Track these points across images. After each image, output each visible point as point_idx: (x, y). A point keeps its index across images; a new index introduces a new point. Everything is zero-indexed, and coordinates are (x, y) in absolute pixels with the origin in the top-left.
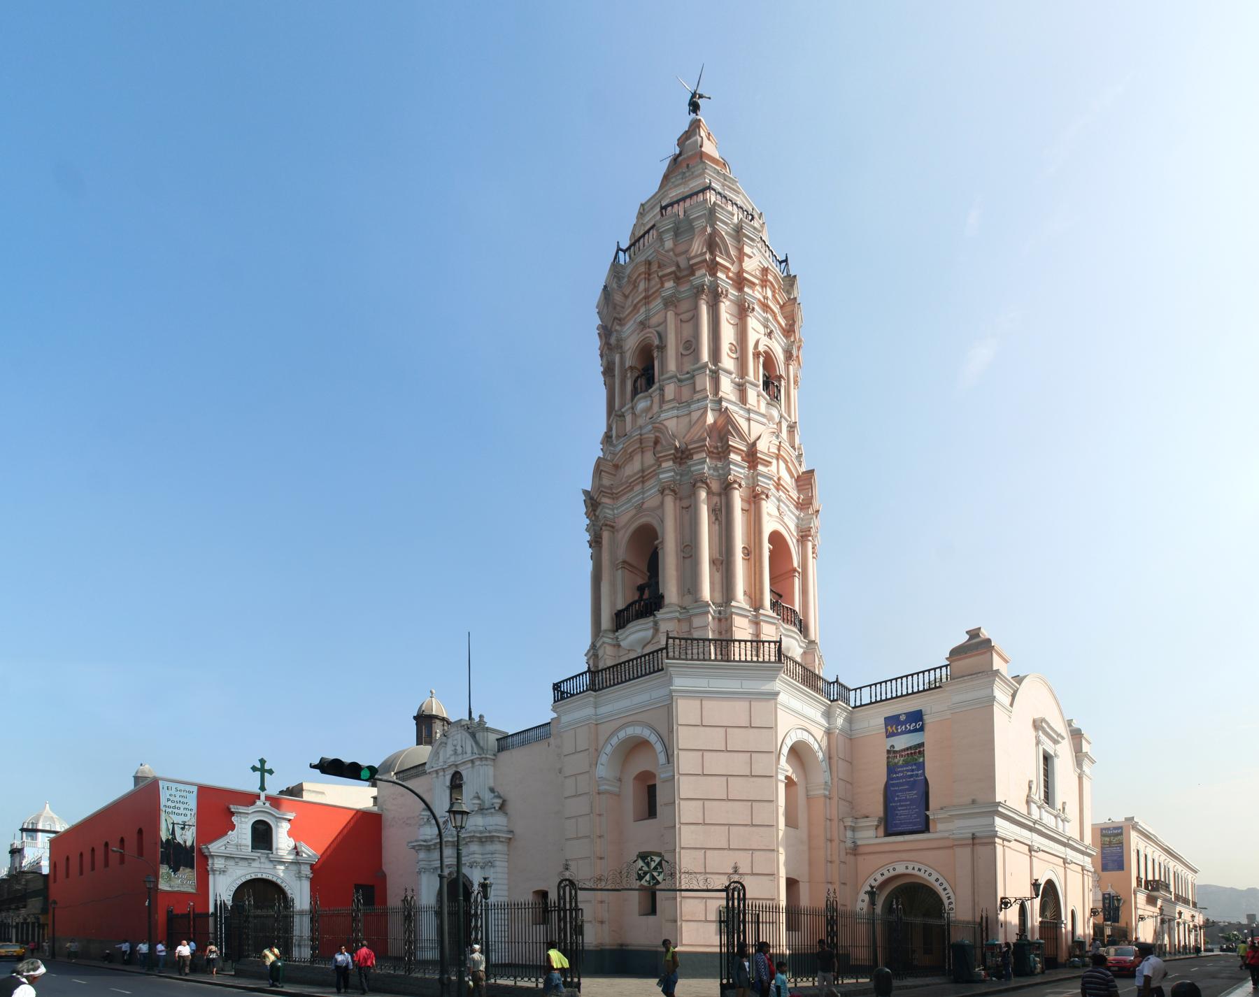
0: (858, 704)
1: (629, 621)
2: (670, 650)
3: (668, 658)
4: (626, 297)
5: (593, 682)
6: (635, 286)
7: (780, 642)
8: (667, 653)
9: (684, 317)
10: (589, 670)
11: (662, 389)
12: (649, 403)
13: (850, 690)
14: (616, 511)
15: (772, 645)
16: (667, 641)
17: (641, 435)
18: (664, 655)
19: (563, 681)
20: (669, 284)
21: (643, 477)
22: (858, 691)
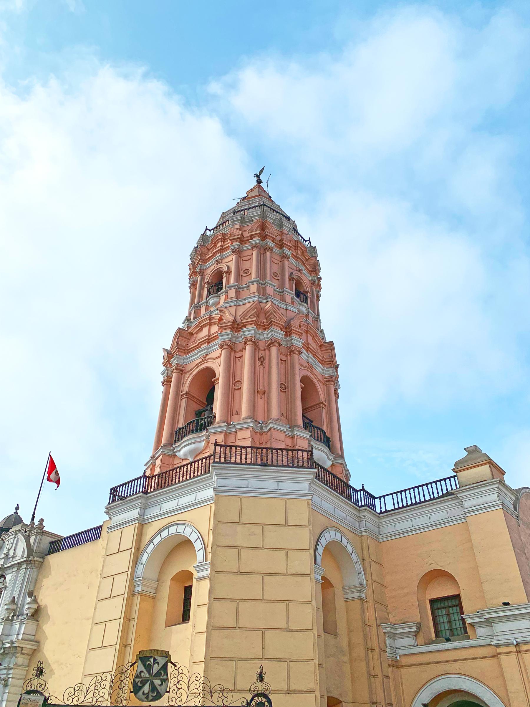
0: (383, 510)
1: (186, 435)
2: (217, 456)
3: (214, 462)
4: (209, 250)
5: (147, 487)
6: (215, 245)
7: (312, 451)
8: (215, 457)
9: (244, 259)
10: (144, 476)
11: (227, 292)
12: (218, 299)
13: (375, 498)
14: (185, 360)
15: (305, 453)
16: (215, 448)
18: (212, 461)
20: (236, 244)
21: (209, 339)
22: (382, 499)
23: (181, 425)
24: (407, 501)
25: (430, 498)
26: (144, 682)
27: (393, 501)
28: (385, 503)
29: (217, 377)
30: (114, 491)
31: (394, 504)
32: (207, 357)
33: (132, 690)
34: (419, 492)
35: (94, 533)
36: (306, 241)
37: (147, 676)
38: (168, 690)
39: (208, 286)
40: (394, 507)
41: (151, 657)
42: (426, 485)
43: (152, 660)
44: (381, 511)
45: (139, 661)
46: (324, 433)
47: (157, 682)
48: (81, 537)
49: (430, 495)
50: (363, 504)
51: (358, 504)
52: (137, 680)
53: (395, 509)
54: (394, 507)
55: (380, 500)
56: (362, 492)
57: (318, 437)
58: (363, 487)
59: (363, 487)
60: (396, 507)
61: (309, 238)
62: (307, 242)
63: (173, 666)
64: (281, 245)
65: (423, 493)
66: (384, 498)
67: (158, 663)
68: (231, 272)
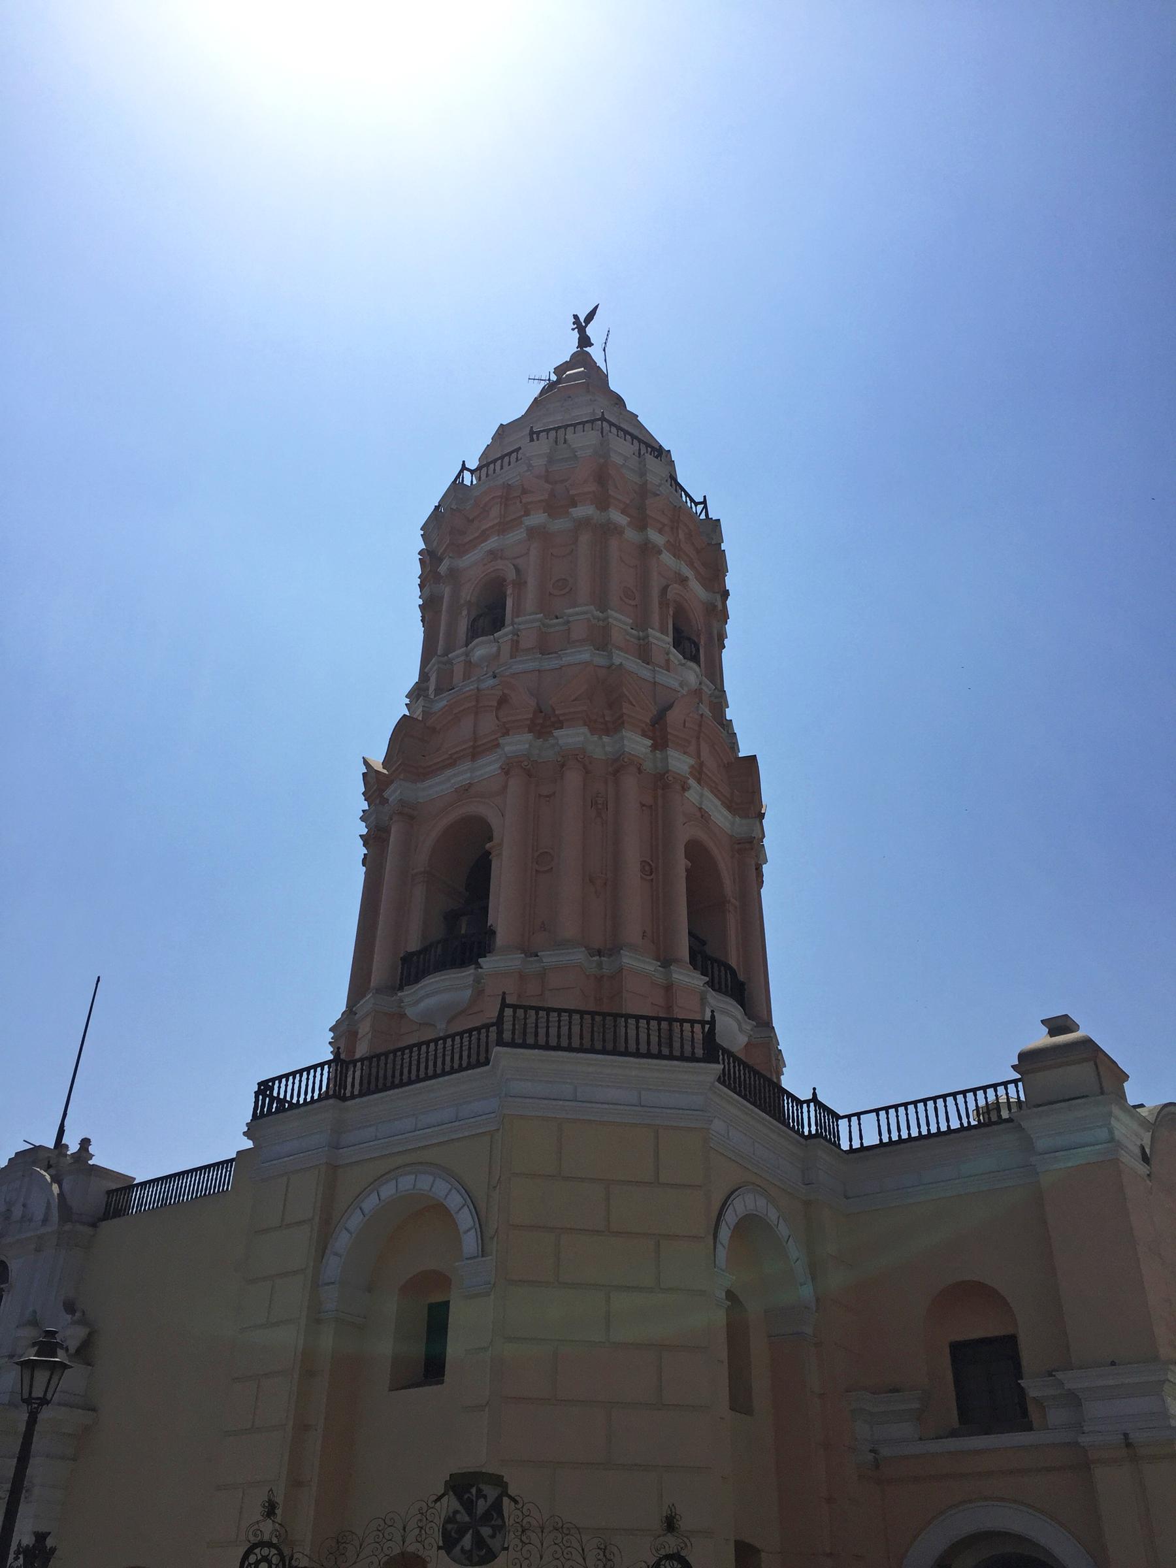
12: (495, 649)
13: (838, 1117)
17: (478, 689)
19: (280, 1078)
23: (414, 945)
24: (909, 1128)
25: (962, 1124)
26: (462, 1532)
27: (879, 1126)
28: (860, 1130)
29: (496, 841)
30: (264, 1088)
31: (880, 1134)
33: (441, 1544)
34: (936, 1109)
35: (213, 1175)
36: (697, 504)
37: (467, 1519)
38: (506, 1545)
39: (469, 614)
40: (881, 1140)
41: (472, 1486)
42: (954, 1095)
43: (474, 1490)
44: (851, 1146)
45: (451, 1493)
46: (733, 973)
47: (486, 1531)
48: (182, 1183)
49: (960, 1118)
50: (814, 1132)
51: (803, 1132)
52: (449, 1526)
53: (882, 1144)
54: (881, 1140)
55: (850, 1121)
56: (812, 1105)
57: (720, 983)
58: (814, 1094)
59: (814, 1094)
60: (885, 1139)
61: (705, 497)
62: (700, 507)
63: (513, 1503)
64: (641, 524)
65: (947, 1113)
66: (859, 1119)
67: (485, 1497)
68: (526, 582)
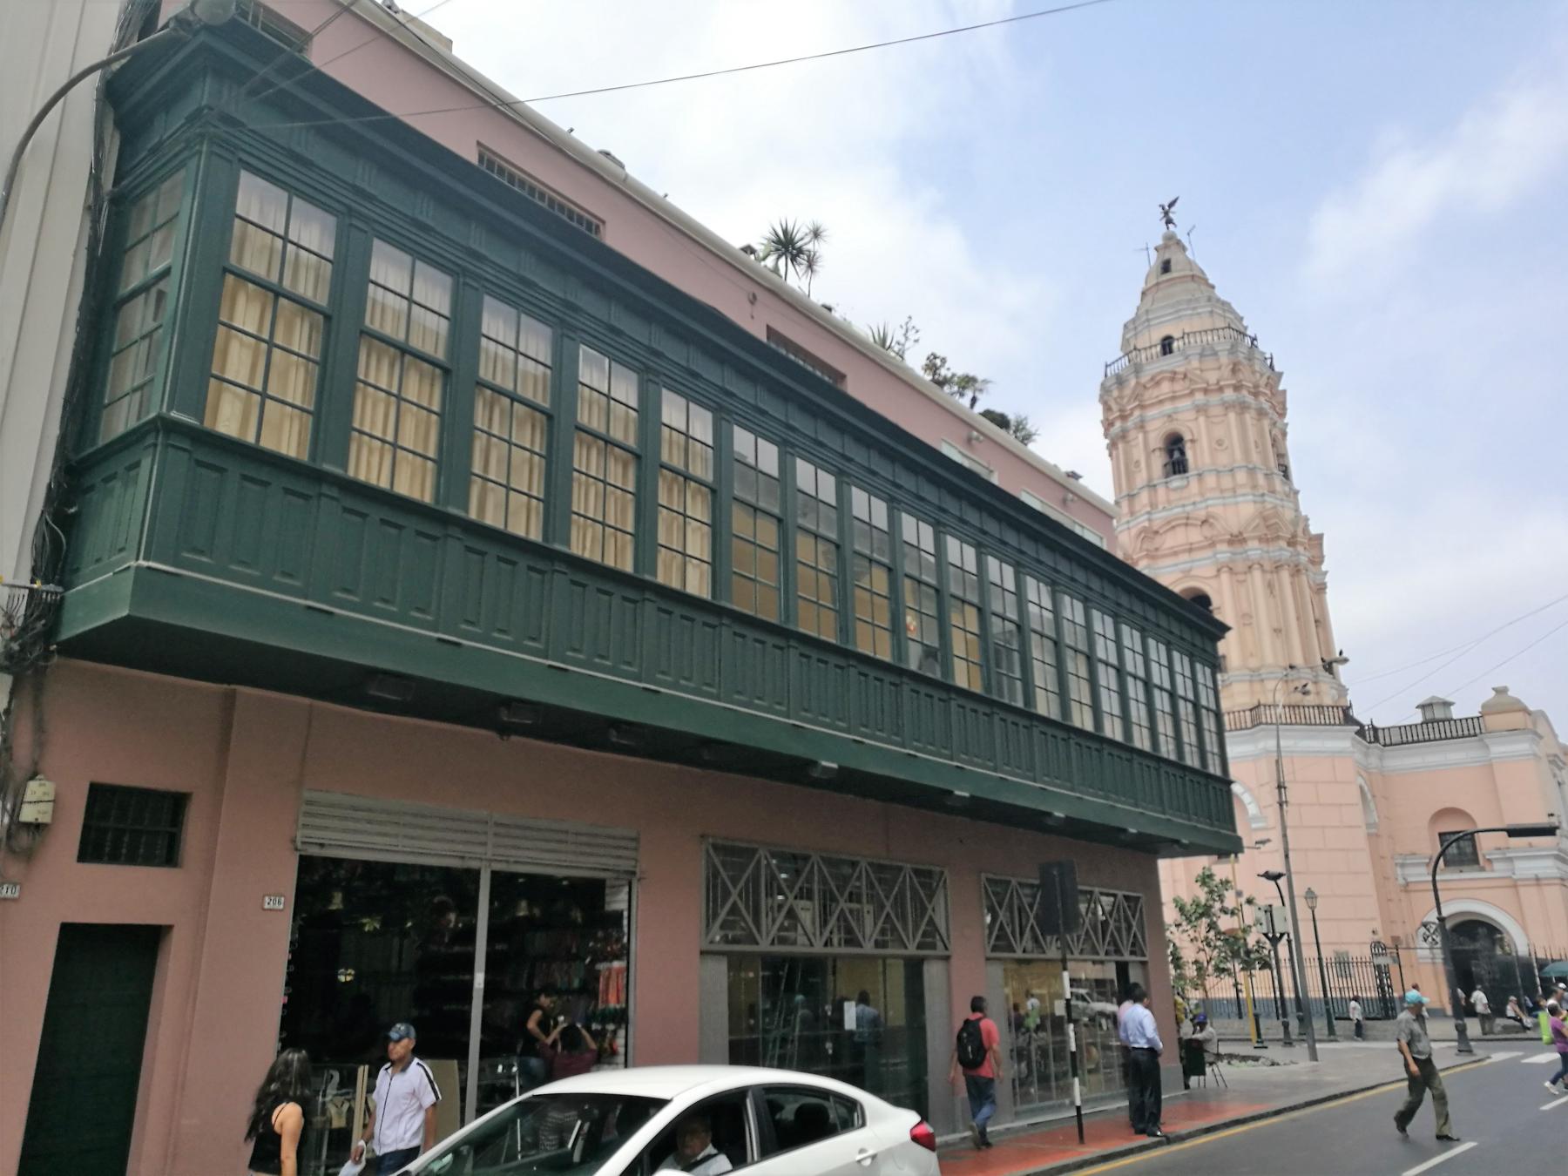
32: (1193, 573)
64: (1256, 395)
